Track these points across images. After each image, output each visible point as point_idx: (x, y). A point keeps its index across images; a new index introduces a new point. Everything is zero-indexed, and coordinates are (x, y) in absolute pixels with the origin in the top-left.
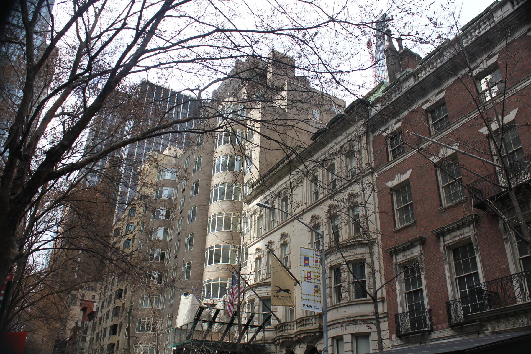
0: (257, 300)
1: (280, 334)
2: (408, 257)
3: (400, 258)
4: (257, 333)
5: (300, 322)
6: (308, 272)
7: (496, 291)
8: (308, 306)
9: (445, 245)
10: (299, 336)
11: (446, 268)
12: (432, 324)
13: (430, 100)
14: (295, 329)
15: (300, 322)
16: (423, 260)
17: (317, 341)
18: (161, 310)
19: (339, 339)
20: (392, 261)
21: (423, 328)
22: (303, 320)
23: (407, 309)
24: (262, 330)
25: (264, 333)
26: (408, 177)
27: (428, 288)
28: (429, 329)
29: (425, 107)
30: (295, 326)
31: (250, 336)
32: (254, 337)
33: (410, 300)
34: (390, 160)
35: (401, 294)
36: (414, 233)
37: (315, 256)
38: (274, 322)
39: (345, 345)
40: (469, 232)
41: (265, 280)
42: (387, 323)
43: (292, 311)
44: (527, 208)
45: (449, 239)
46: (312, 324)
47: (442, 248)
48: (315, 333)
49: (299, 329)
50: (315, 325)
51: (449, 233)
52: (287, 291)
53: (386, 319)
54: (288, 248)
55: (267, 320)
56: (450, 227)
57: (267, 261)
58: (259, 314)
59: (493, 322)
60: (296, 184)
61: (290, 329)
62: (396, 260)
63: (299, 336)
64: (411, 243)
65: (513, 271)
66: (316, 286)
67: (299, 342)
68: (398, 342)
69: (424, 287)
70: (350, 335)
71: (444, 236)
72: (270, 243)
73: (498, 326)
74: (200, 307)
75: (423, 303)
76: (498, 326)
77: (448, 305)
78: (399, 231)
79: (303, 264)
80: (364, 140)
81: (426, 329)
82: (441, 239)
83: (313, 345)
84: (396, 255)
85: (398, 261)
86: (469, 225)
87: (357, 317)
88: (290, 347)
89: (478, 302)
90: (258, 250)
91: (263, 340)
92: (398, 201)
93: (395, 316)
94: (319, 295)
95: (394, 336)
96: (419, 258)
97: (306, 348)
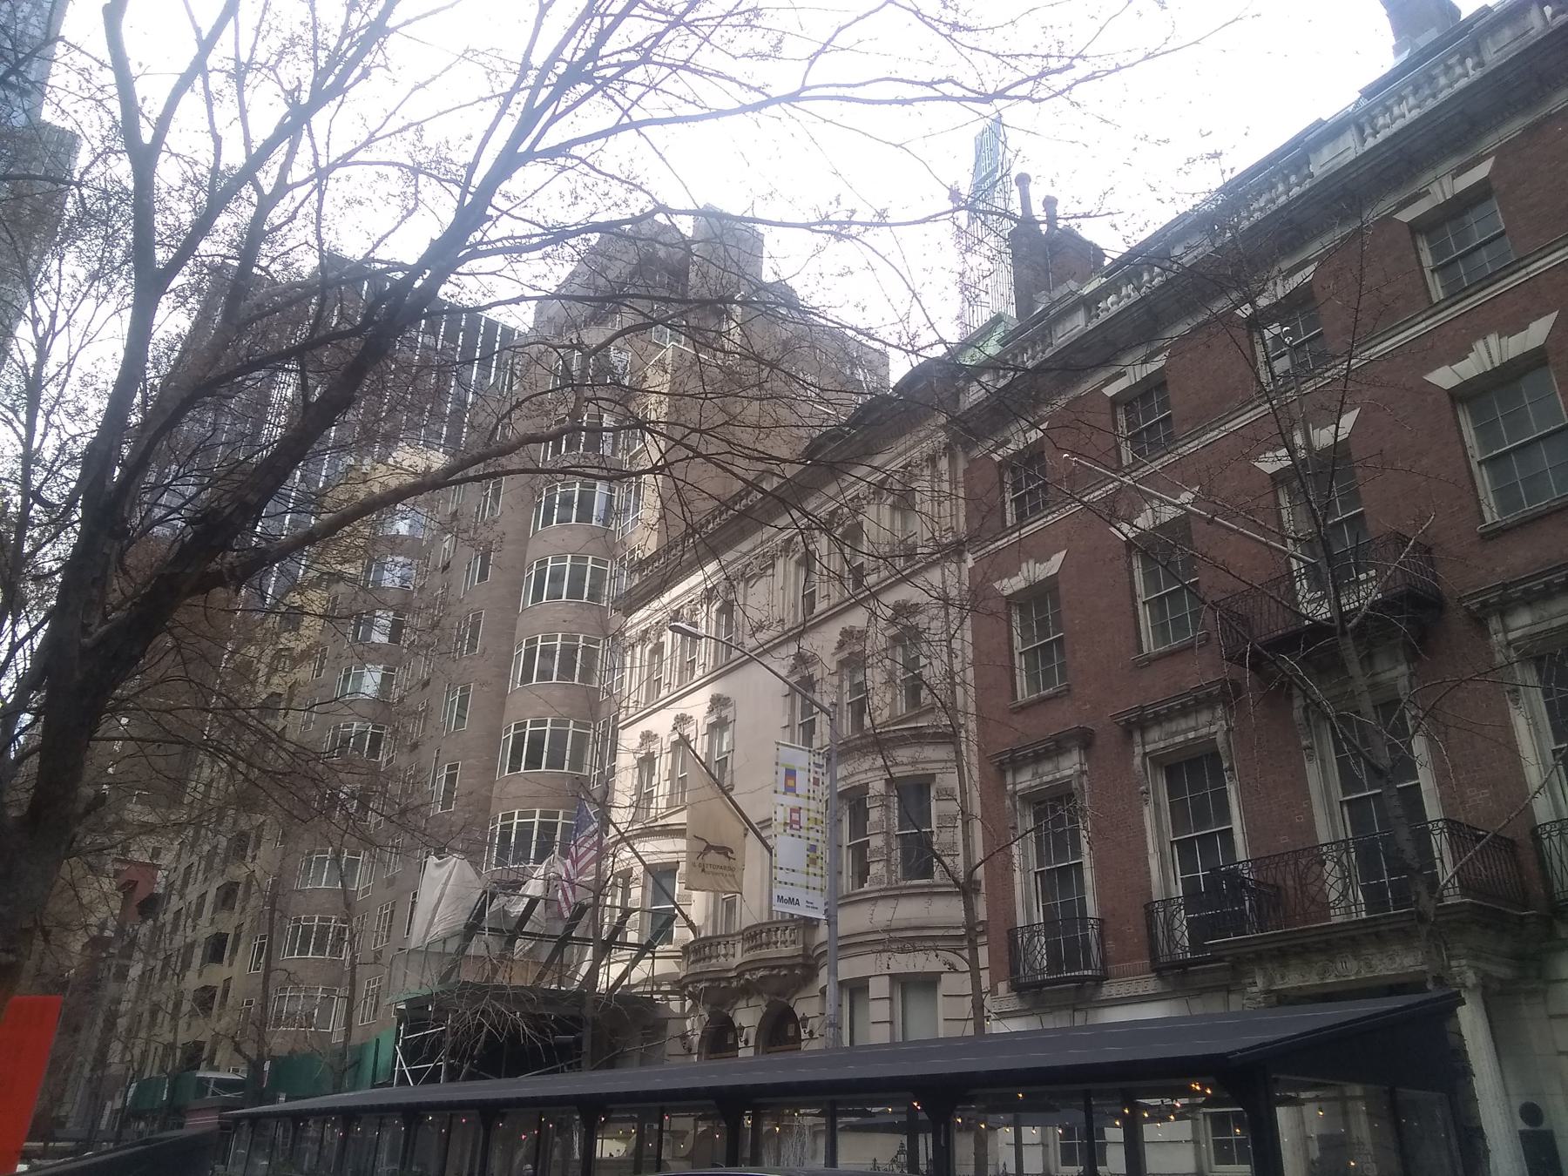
0: (638, 870)
1: (698, 968)
2: (1045, 779)
3: (1025, 780)
4: (634, 962)
5: (753, 935)
6: (793, 810)
7: (1281, 883)
8: (791, 901)
9: (1145, 754)
10: (747, 976)
11: (1148, 813)
12: (1104, 961)
13: (1124, 374)
14: (739, 955)
15: (753, 937)
16: (1086, 787)
17: (797, 992)
18: (360, 894)
19: (857, 989)
20: (1005, 786)
21: (1080, 969)
22: (762, 932)
23: (1039, 917)
26: (1054, 571)
27: (1099, 865)
29: (1110, 391)
30: (739, 947)
31: (616, 970)
32: (625, 974)
33: (1047, 893)
34: (1009, 524)
36: (1064, 717)
37: (812, 768)
38: (681, 934)
39: (873, 1005)
40: (1210, 726)
41: (662, 818)
43: (730, 906)
45: (1157, 740)
46: (784, 942)
47: (1137, 761)
48: (791, 968)
49: (749, 956)
50: (793, 947)
51: (1160, 724)
52: (724, 851)
54: (727, 736)
55: (662, 927)
56: (1162, 709)
57: (669, 767)
58: (642, 910)
59: (1269, 966)
60: (756, 570)
61: (725, 956)
62: (1014, 784)
63: (747, 976)
64: (1057, 742)
65: (1324, 836)
66: (813, 848)
67: (747, 991)
68: (1013, 1004)
69: (1086, 861)
71: (1144, 730)
72: (682, 720)
73: (1283, 978)
74: (485, 892)
75: (1082, 901)
76: (1283, 978)
77: (1149, 909)
78: (1023, 708)
79: (781, 788)
80: (944, 464)
81: (1090, 973)
82: (1137, 738)
83: (784, 1000)
84: (1016, 770)
85: (1018, 787)
86: (1212, 708)
87: (906, 929)
90: (648, 737)
92: (1026, 628)
93: (1008, 931)
94: (819, 872)
95: (1002, 987)
96: (1075, 784)
97: (765, 1009)
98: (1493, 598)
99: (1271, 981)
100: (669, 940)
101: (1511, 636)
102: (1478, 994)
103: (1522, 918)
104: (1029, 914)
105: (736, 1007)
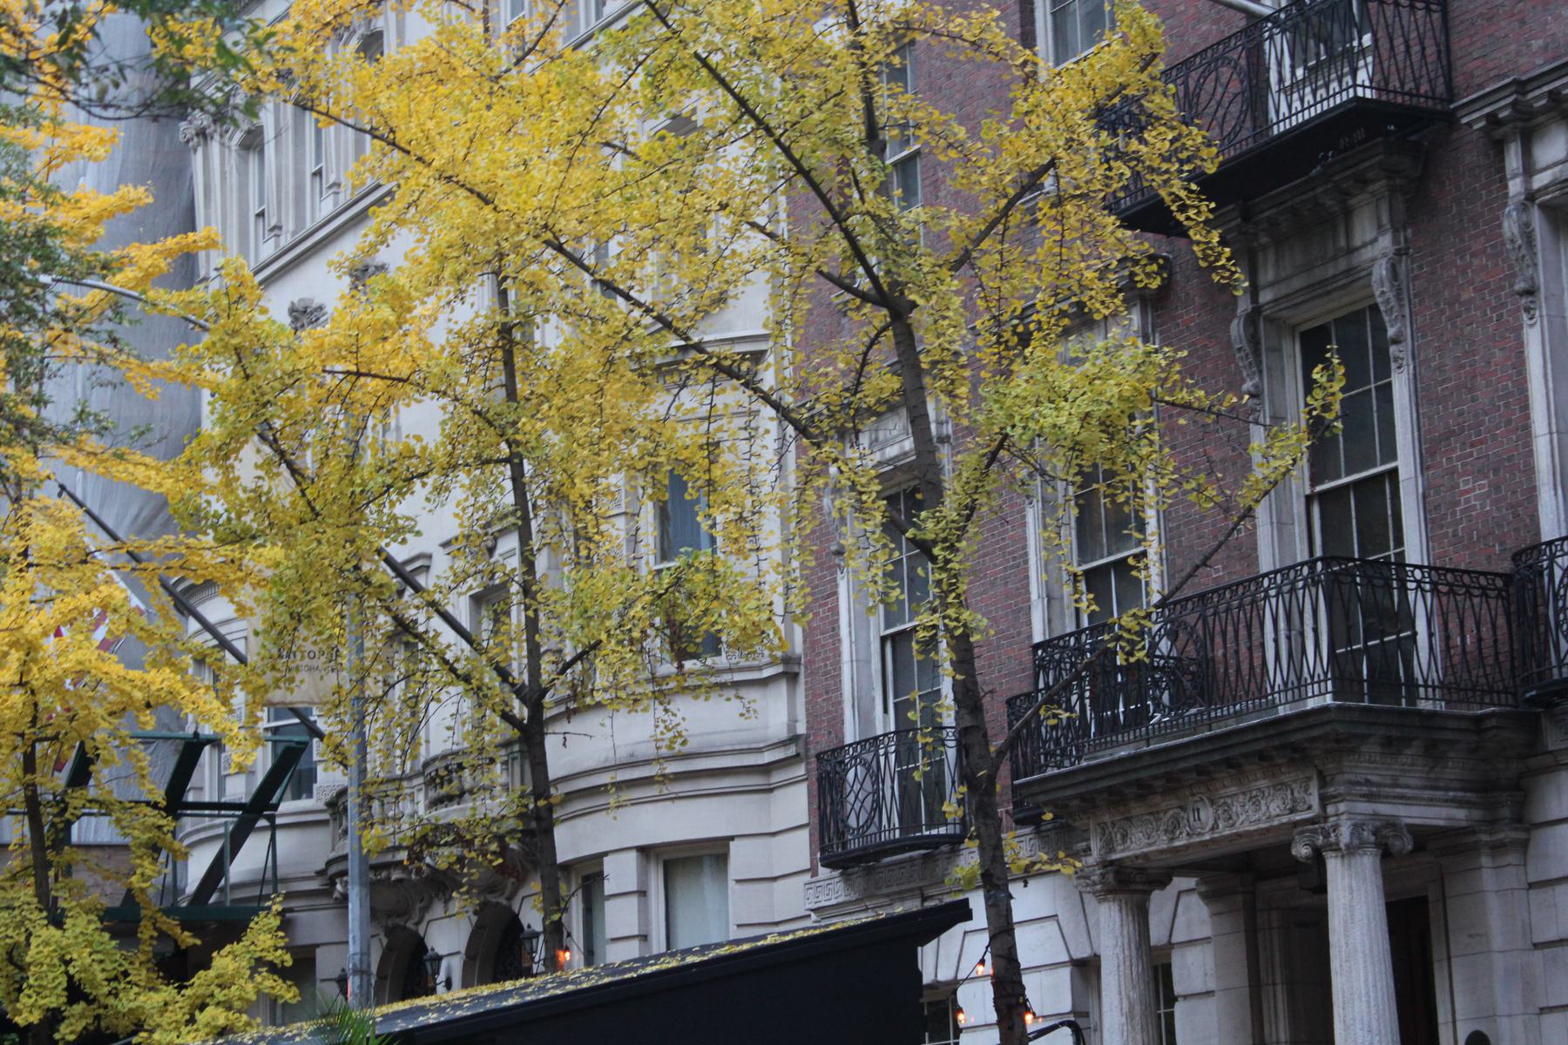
4: (236, 841)
19: (589, 874)
22: (461, 767)
23: (884, 723)
24: (262, 823)
25: (273, 840)
28: (951, 830)
32: (218, 869)
35: (859, 641)
38: (329, 778)
42: (803, 788)
44: (1342, 242)
53: (800, 770)
59: (1107, 818)
68: (833, 889)
70: (633, 855)
73: (1124, 837)
81: (942, 830)
83: (503, 901)
88: (405, 912)
89: (1366, 640)
91: (269, 874)
98: (1503, 107)
99: (1109, 846)
100: (304, 786)
101: (1540, 181)
102: (1368, 863)
103: (1479, 719)
104: (865, 717)
105: (428, 917)
